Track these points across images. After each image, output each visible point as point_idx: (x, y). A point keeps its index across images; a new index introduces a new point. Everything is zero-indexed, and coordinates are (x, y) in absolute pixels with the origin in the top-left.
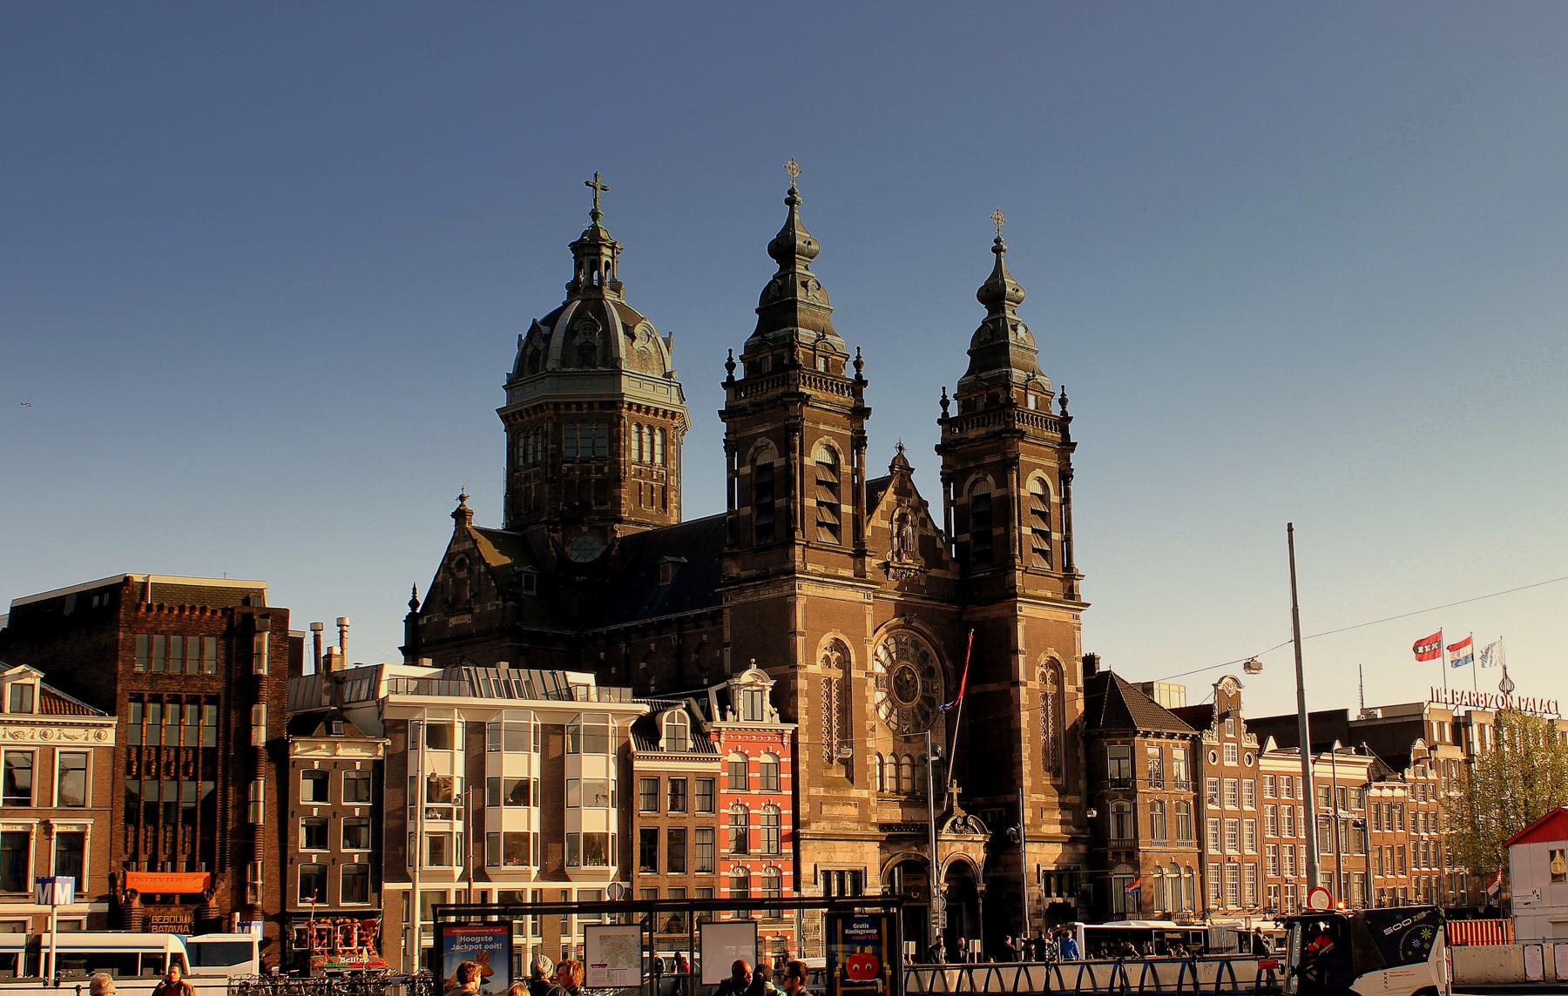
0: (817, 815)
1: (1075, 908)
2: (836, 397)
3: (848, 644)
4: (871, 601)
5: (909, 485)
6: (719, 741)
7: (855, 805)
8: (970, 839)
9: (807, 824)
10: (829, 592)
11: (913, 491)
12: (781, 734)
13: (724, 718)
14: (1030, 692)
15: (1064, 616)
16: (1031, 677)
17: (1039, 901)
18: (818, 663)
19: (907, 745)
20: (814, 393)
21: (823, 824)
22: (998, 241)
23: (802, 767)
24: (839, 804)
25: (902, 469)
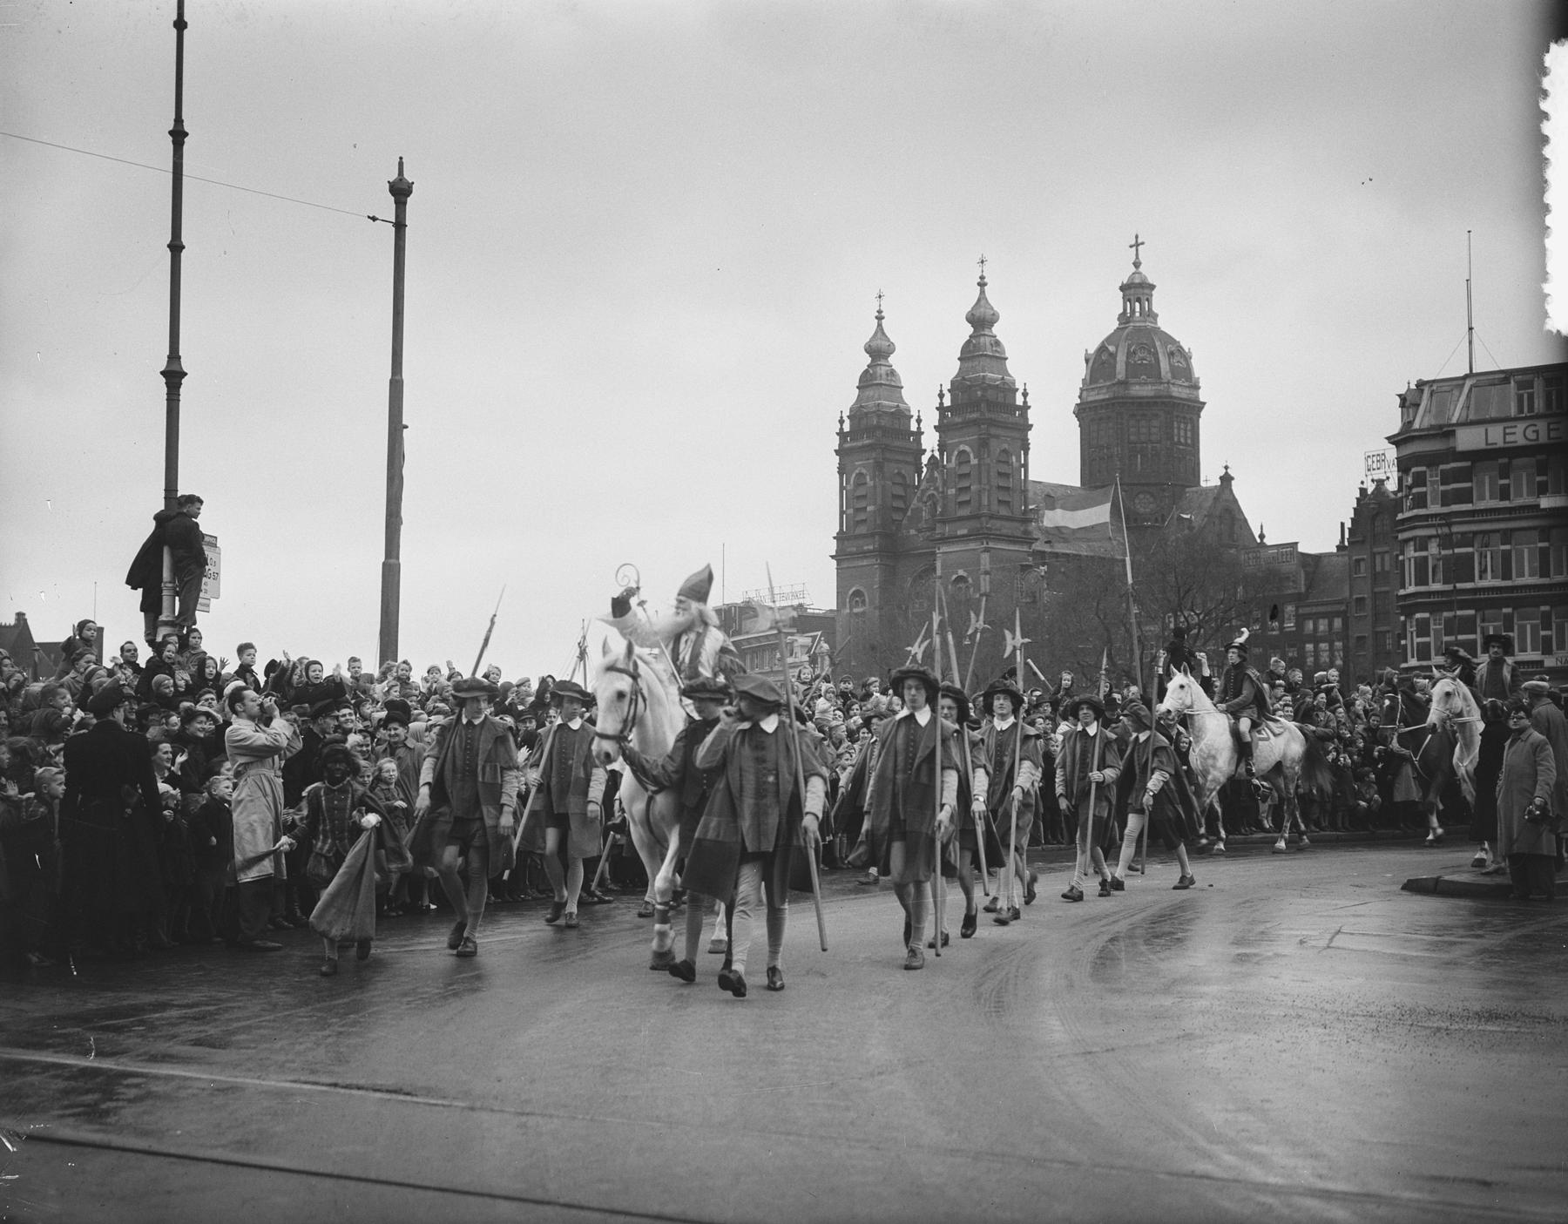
22: (982, 278)
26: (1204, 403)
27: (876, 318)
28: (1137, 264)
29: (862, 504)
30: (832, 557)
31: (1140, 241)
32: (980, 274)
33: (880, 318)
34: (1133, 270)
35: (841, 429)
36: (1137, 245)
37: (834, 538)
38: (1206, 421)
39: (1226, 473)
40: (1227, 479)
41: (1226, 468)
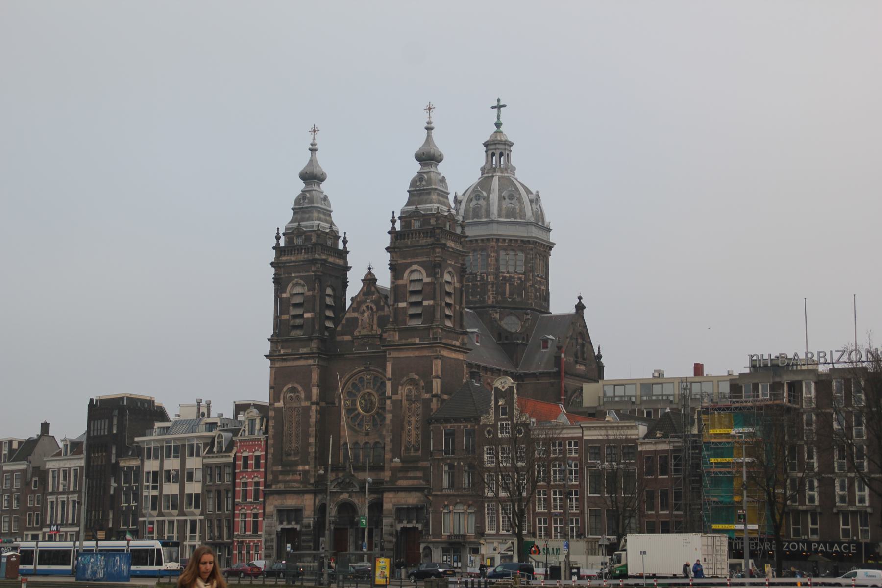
0: (276, 481)
1: (422, 531)
2: (303, 256)
3: (300, 388)
4: (316, 363)
5: (373, 289)
6: (237, 446)
7: (300, 475)
8: (350, 490)
9: (270, 486)
10: (289, 364)
11: (376, 292)
12: (259, 440)
13: (241, 435)
14: (394, 403)
15: (426, 353)
16: (395, 391)
17: (392, 526)
18: (282, 401)
19: (366, 437)
20: (289, 258)
21: (279, 485)
23: (269, 456)
24: (289, 475)
25: (370, 280)
26: (554, 244)
27: (310, 150)
28: (498, 125)
29: (299, 311)
30: (267, 356)
31: (501, 104)
32: (428, 120)
33: (313, 150)
34: (495, 129)
35: (278, 244)
36: (499, 107)
37: (269, 339)
38: (555, 259)
39: (580, 303)
40: (580, 307)
41: (580, 298)
